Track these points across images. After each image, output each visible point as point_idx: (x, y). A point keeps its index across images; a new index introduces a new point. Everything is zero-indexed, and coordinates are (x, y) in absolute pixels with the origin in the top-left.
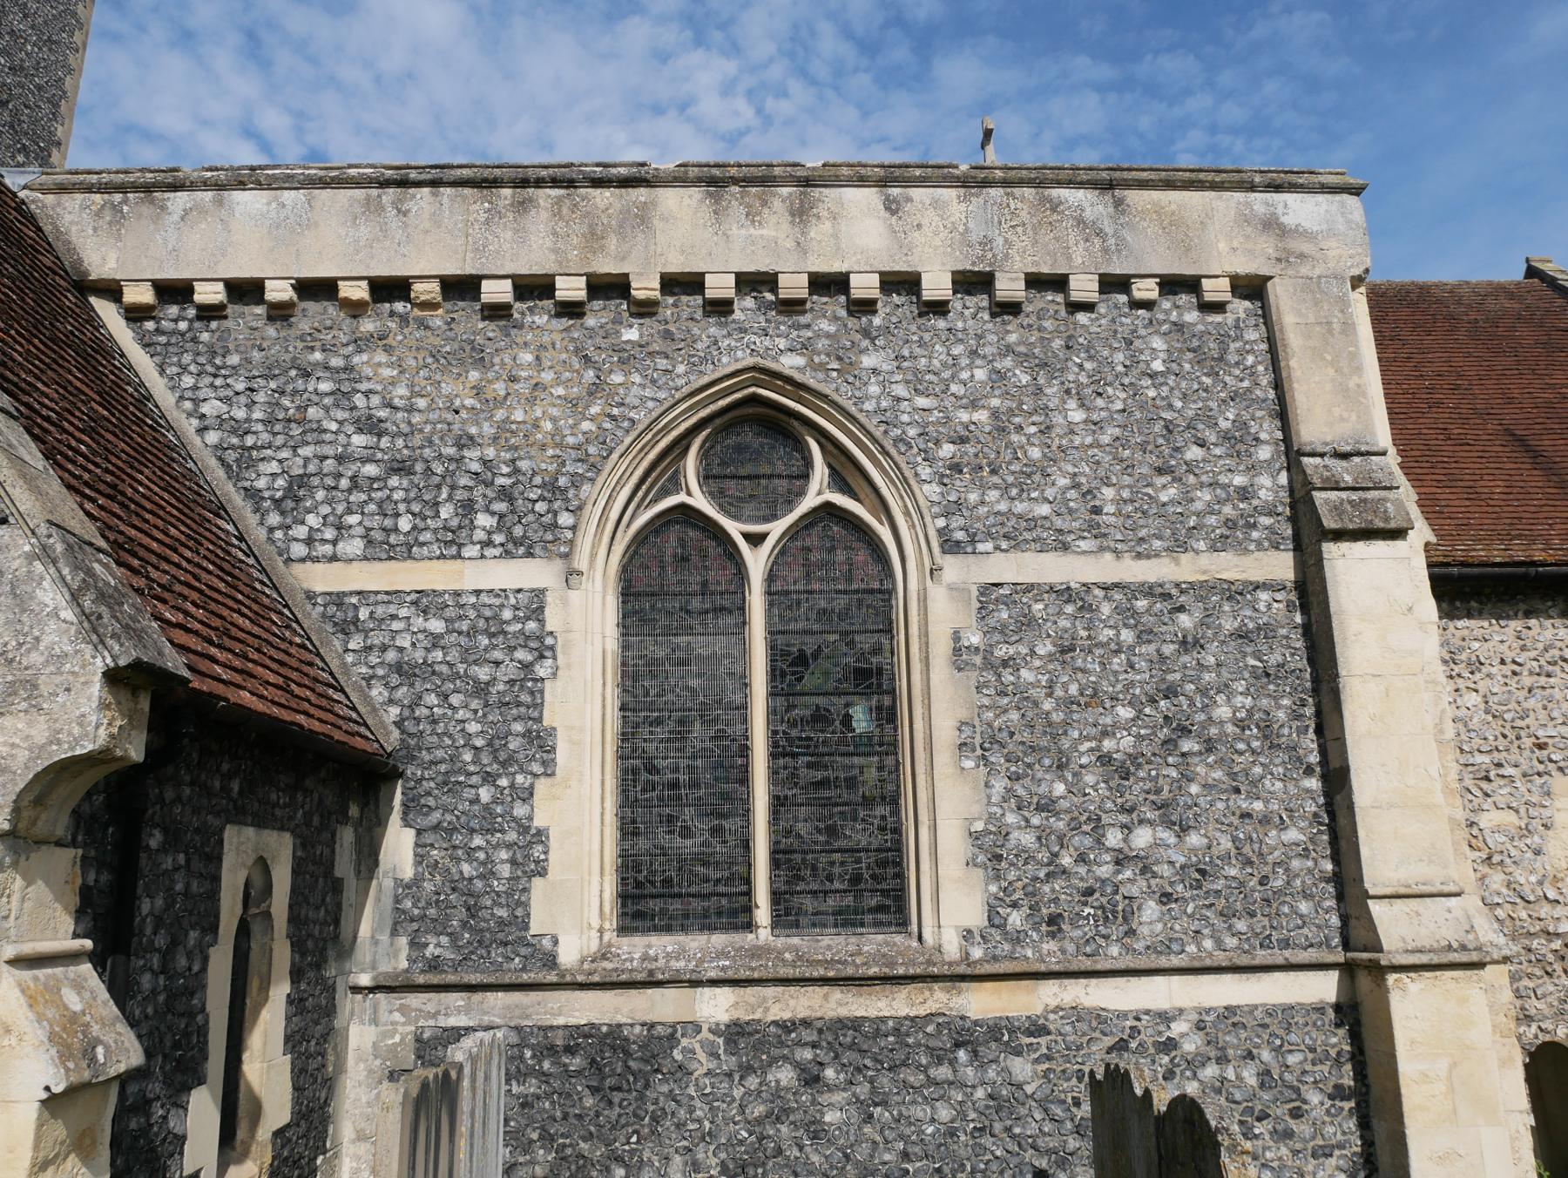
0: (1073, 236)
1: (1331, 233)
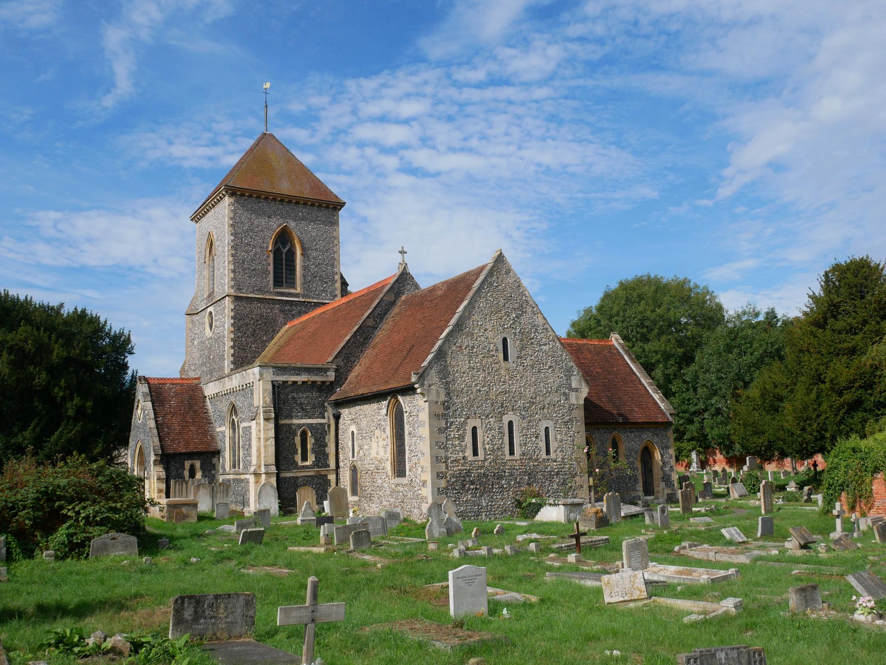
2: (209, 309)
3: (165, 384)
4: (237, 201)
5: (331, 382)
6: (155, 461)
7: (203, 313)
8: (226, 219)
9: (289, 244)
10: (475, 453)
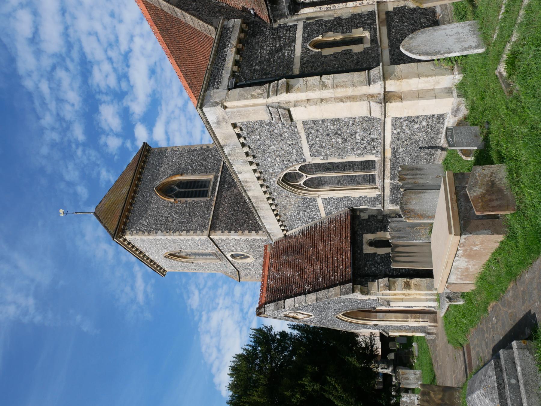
0: (235, 152)
1: (215, 114)
2: (230, 258)
3: (268, 284)
4: (130, 228)
5: (243, 23)
6: (362, 292)
7: (235, 265)
8: (144, 238)
9: (173, 186)
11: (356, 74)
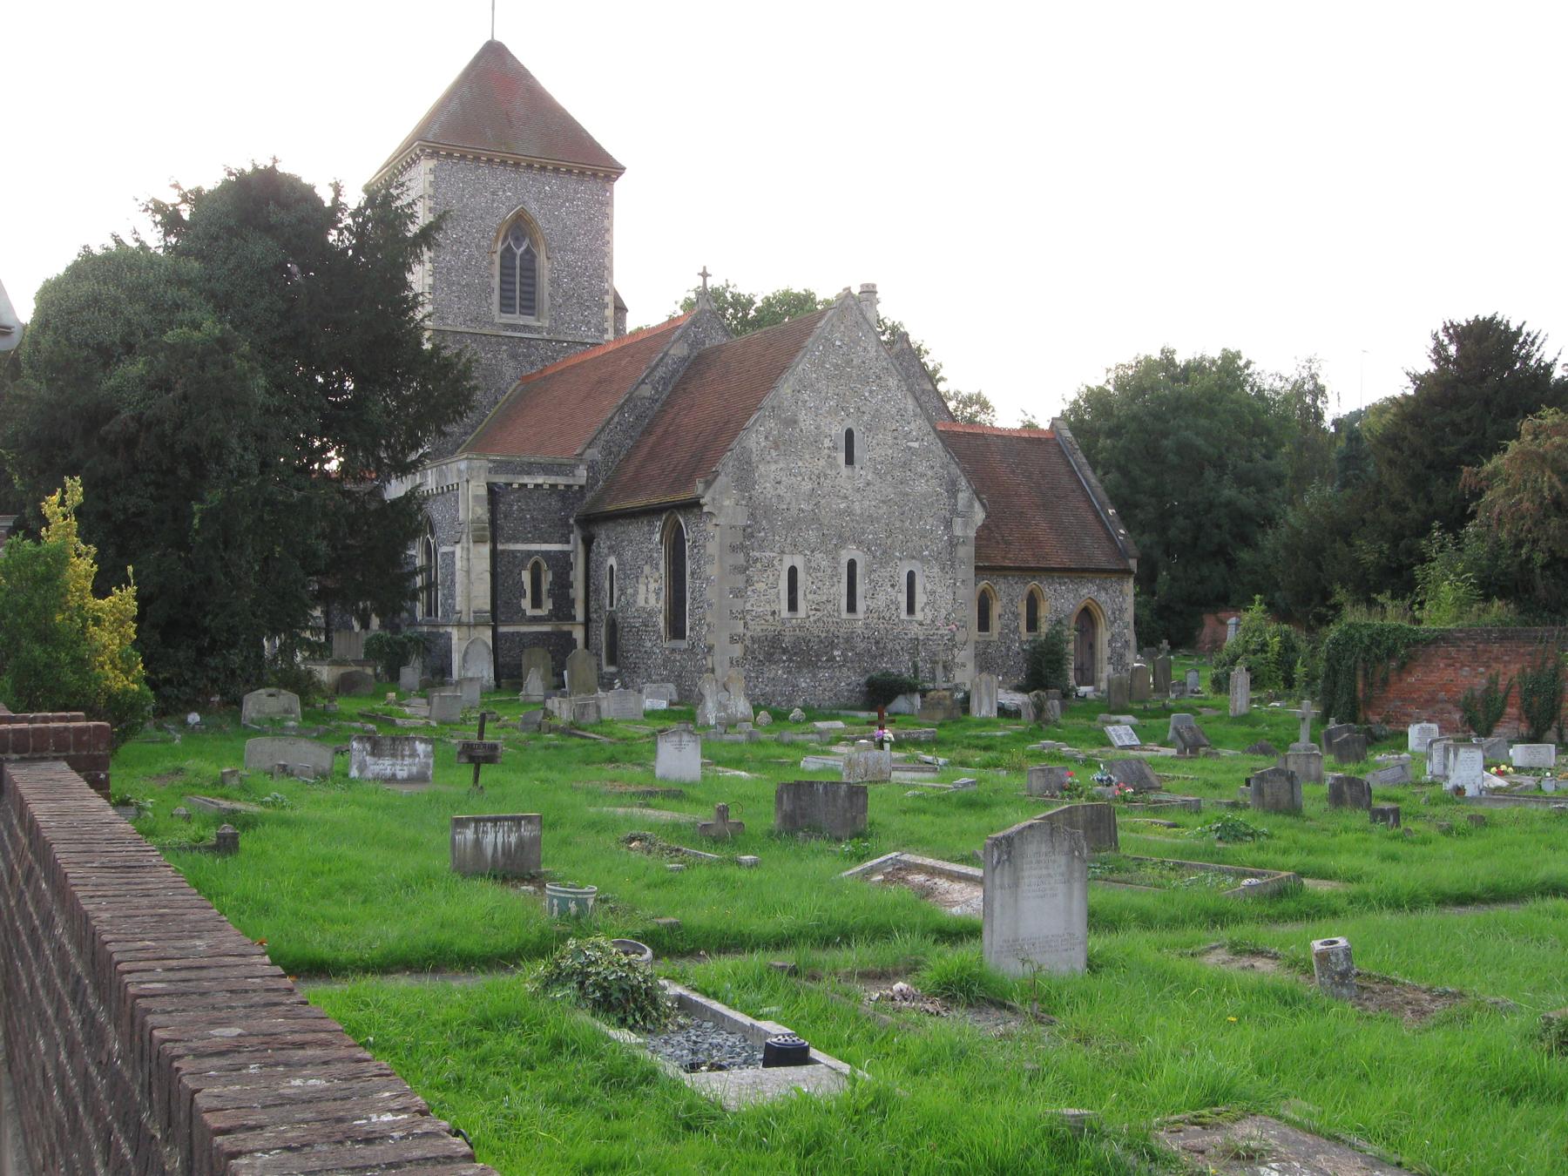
9: (527, 240)
10: (793, 606)
11: (488, 601)
